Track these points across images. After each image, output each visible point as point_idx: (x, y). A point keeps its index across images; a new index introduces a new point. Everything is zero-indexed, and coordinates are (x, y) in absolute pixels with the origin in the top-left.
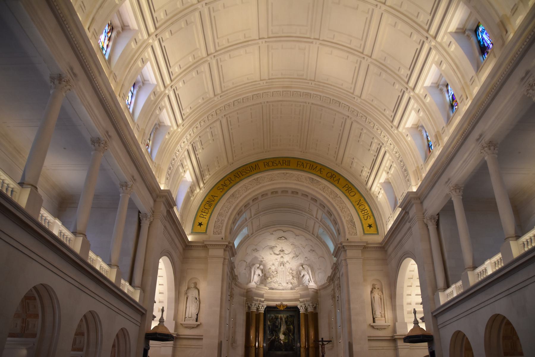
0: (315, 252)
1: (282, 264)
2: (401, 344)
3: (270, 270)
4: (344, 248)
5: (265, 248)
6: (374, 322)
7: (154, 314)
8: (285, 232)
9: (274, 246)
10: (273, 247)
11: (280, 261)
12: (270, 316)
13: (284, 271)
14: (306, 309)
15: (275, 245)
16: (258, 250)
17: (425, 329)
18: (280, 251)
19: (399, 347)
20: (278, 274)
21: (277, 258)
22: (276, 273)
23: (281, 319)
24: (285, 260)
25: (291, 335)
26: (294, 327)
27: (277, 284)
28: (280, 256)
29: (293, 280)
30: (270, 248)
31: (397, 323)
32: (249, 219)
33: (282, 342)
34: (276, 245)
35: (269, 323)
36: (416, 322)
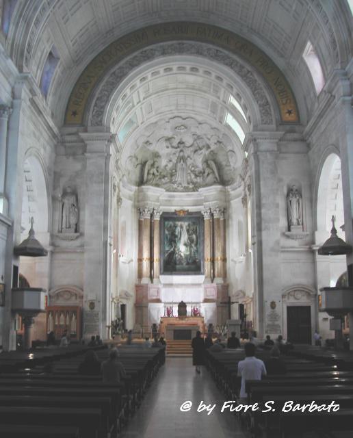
2: (319, 258)
4: (255, 140)
6: (289, 230)
7: (22, 225)
8: (185, 119)
12: (168, 224)
14: (212, 215)
17: (344, 239)
18: (179, 143)
19: (317, 260)
22: (174, 171)
23: (181, 227)
24: (186, 156)
25: (193, 245)
26: (197, 238)
28: (179, 150)
31: (316, 232)
32: (137, 104)
33: (182, 255)
34: (175, 136)
35: (167, 232)
36: (334, 231)
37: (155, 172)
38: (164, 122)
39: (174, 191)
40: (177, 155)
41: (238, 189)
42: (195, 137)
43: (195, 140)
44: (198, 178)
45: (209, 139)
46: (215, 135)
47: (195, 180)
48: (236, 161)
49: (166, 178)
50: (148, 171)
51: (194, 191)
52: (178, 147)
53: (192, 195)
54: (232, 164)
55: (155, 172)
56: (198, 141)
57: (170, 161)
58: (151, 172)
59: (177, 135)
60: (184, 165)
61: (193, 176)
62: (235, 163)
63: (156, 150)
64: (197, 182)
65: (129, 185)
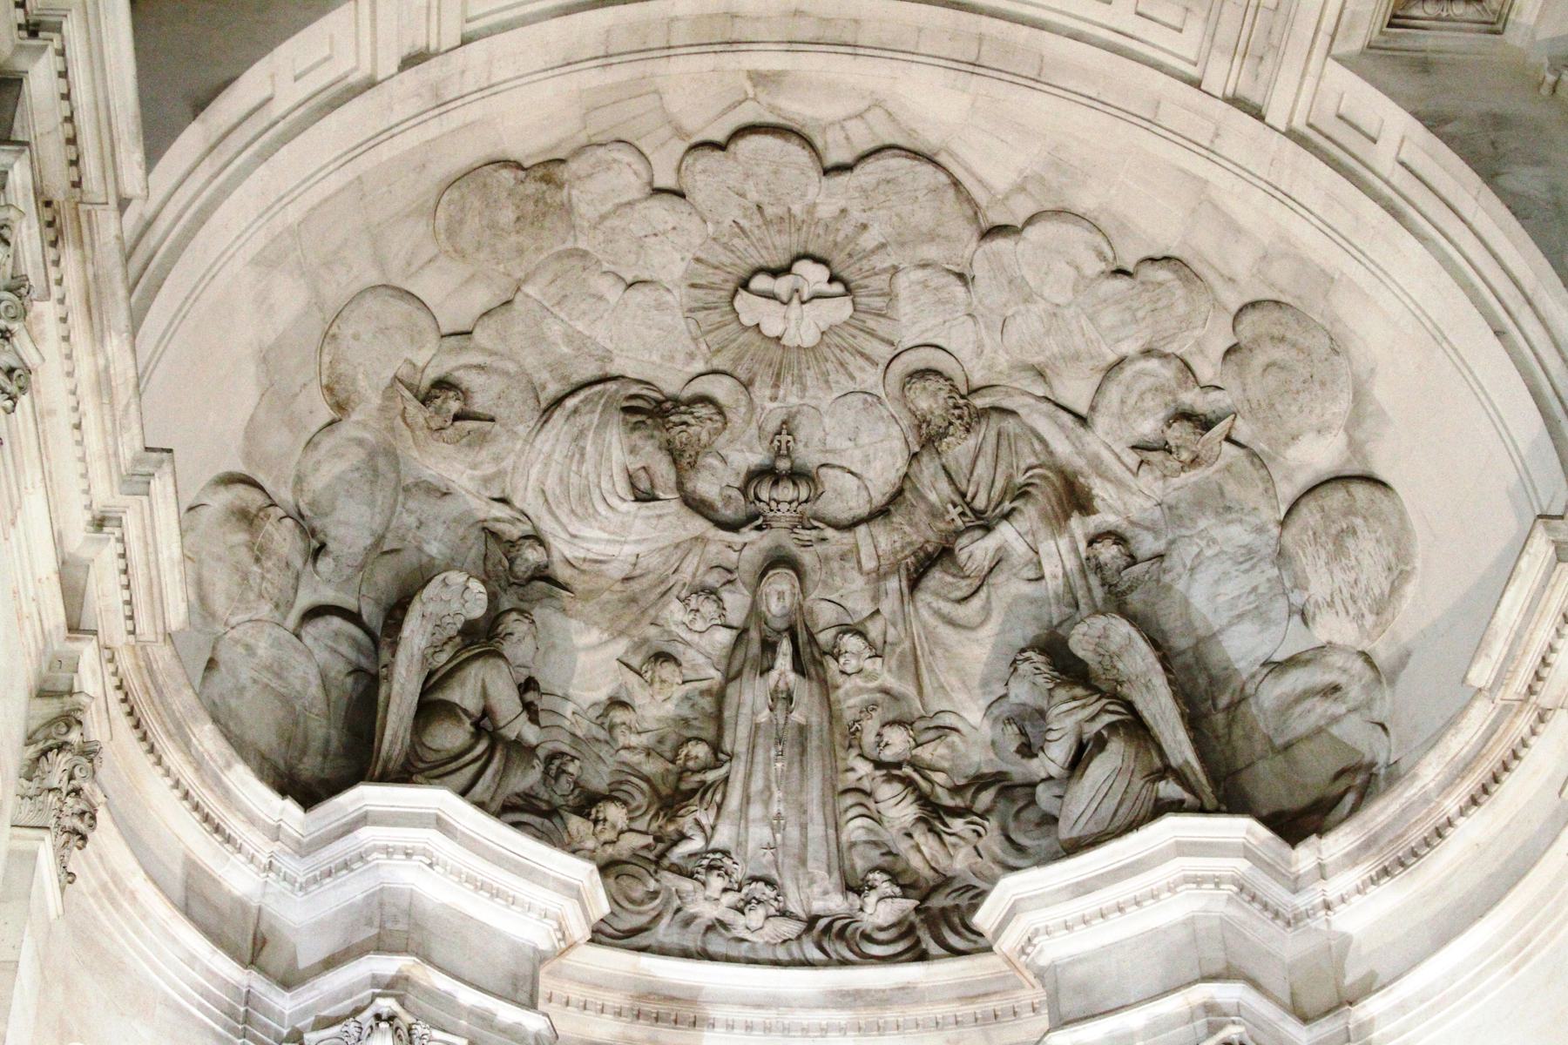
0: (1228, 439)
1: (785, 647)
3: (619, 716)
5: (571, 403)
9: (688, 393)
10: (676, 401)
11: (755, 611)
13: (802, 730)
15: (701, 386)
16: (479, 404)
18: (765, 474)
20: (738, 770)
21: (713, 579)
24: (826, 614)
27: (716, 882)
29: (928, 843)
30: (626, 410)
34: (720, 389)
37: (506, 703)
38: (624, 178)
39: (705, 955)
40: (736, 603)
41: (1472, 831)
42: (928, 400)
43: (928, 439)
44: (957, 824)
45: (1082, 420)
46: (1147, 353)
47: (923, 854)
48: (1399, 574)
49: (614, 813)
50: (434, 682)
51: (923, 957)
52: (754, 520)
53: (905, 993)
54: (1332, 628)
55: (506, 703)
56: (959, 448)
57: (662, 657)
58: (464, 694)
59: (747, 385)
60: (804, 691)
61: (900, 811)
62: (1381, 607)
63: (527, 500)
64: (944, 881)
65: (207, 737)
